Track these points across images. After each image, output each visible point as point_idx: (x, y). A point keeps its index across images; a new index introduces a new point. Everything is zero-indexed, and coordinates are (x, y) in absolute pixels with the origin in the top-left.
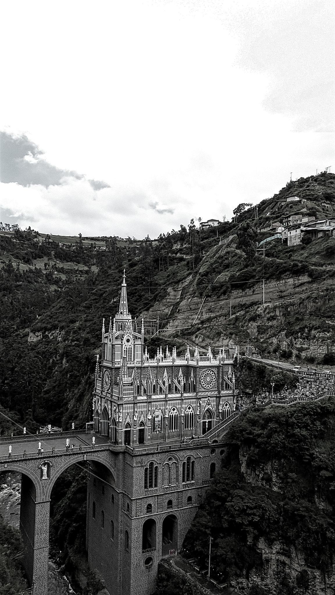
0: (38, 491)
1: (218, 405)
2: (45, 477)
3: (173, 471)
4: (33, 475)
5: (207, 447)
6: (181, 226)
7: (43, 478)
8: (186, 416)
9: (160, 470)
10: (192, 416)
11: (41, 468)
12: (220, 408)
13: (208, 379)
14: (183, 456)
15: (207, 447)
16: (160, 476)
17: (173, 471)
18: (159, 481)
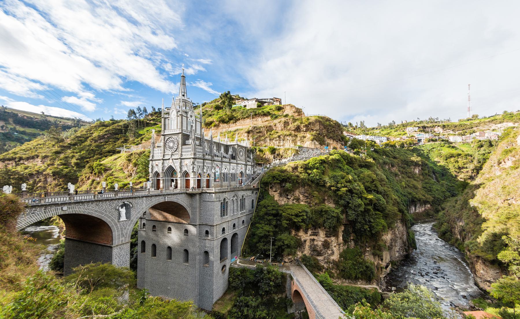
0: (116, 234)
1: (246, 170)
2: (123, 218)
3: (235, 204)
4: (109, 217)
5: (251, 189)
6: (153, 107)
7: (121, 220)
8: (232, 174)
9: (229, 203)
10: (234, 174)
11: (118, 210)
12: (247, 171)
13: (241, 154)
14: (240, 194)
15: (251, 189)
16: (229, 208)
17: (235, 204)
18: (229, 211)
